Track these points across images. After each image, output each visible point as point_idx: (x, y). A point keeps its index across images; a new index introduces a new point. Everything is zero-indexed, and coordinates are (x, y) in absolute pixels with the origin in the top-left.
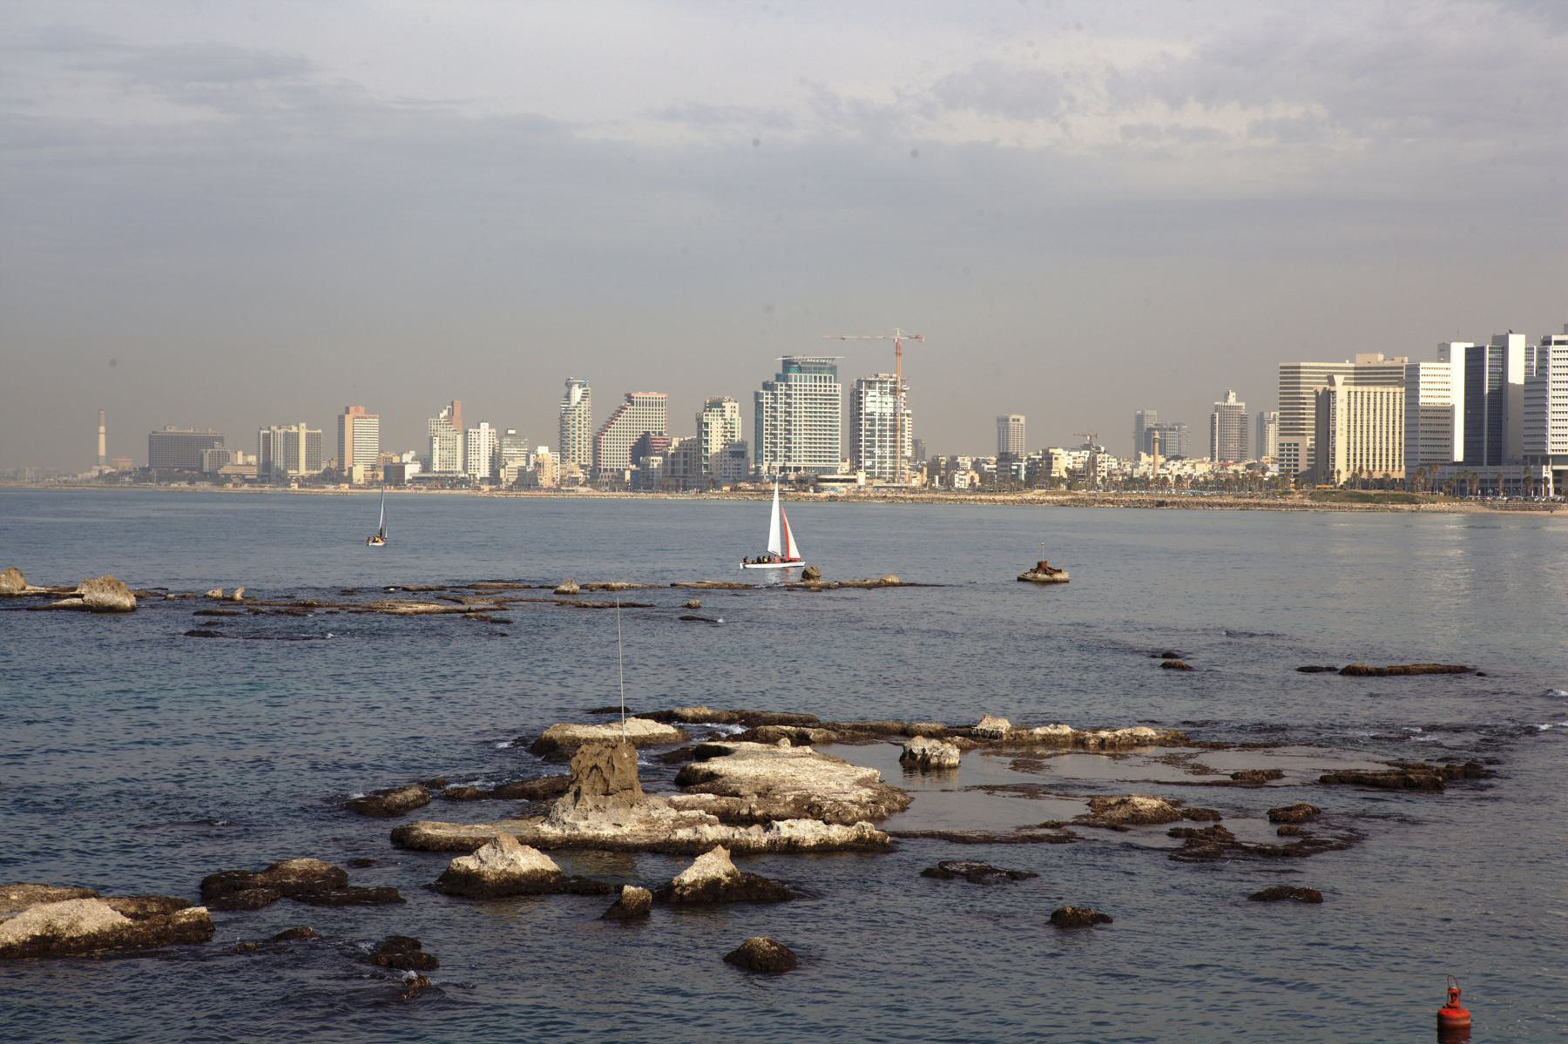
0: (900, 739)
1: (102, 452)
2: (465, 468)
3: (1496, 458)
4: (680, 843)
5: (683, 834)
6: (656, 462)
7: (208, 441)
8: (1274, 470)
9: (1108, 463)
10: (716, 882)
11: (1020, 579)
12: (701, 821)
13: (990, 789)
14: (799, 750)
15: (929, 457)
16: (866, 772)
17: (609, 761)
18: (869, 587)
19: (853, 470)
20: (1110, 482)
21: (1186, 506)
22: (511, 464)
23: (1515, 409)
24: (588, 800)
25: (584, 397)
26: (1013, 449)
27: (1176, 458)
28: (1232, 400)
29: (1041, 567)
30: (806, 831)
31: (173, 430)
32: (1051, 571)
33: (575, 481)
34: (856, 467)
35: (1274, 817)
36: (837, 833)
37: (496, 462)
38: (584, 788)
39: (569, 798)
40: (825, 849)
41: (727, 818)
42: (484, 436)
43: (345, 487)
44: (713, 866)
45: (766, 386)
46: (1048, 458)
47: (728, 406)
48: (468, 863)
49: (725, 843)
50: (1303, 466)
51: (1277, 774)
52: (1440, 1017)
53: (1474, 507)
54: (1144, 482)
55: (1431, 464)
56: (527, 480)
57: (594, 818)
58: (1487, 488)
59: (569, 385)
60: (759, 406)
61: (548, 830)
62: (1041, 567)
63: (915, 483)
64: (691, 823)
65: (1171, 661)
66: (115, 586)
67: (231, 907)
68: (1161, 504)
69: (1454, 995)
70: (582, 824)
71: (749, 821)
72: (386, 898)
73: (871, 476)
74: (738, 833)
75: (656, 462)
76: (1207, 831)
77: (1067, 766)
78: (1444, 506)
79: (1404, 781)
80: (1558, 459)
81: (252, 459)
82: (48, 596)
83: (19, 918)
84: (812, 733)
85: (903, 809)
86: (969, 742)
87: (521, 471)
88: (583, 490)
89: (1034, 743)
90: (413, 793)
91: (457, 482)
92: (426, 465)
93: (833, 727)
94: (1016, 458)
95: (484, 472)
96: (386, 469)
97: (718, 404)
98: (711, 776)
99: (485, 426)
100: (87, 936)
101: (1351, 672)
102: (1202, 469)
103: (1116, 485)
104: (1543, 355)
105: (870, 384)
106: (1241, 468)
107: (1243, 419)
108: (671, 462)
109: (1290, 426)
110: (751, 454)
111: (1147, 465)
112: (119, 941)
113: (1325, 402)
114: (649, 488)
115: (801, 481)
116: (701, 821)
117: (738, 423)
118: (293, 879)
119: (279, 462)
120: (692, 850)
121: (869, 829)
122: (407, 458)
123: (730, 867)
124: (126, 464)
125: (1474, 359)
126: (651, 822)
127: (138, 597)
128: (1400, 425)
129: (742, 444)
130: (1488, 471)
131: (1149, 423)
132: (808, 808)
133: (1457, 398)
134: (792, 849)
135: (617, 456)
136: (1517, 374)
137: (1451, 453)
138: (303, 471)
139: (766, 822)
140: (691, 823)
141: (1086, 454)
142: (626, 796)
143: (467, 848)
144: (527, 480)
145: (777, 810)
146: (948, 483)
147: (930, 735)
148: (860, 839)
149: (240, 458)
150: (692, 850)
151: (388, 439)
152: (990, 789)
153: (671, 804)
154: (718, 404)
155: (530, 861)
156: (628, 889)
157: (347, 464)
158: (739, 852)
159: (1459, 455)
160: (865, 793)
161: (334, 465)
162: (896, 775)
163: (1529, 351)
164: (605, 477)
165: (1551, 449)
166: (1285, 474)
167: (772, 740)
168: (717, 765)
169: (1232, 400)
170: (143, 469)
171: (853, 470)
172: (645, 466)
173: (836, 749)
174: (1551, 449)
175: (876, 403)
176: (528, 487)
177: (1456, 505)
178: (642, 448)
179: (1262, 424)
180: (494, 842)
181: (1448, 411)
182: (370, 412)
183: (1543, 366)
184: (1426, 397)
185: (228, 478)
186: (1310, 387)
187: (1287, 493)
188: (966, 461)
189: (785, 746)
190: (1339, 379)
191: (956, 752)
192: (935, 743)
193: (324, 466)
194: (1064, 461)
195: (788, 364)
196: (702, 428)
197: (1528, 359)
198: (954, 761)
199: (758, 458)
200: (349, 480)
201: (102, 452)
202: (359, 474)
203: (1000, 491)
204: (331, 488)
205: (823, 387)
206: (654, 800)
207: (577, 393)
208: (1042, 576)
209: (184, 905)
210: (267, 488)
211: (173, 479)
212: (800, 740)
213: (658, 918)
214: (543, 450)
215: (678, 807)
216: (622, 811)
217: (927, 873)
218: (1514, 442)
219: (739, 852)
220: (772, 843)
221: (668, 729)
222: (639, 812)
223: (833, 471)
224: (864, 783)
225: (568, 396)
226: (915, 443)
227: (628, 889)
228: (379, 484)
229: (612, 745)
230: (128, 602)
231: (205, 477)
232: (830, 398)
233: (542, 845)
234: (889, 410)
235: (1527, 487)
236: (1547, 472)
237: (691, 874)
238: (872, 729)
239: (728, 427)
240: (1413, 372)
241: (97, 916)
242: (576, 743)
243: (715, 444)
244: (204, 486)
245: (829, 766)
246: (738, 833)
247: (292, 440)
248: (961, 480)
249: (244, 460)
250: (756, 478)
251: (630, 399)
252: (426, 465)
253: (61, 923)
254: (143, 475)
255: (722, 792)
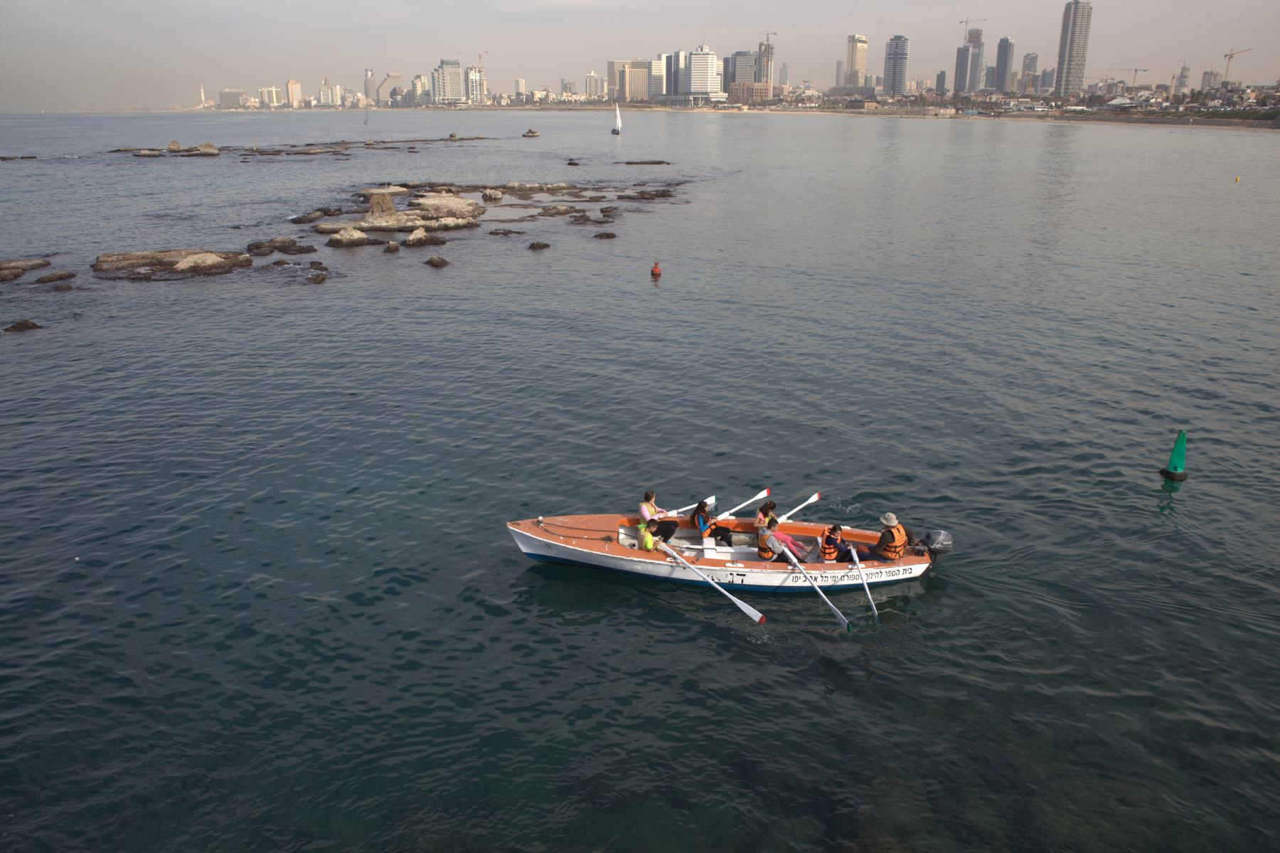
0: (482, 190)
1: (203, 98)
2: (333, 102)
3: (676, 93)
4: (409, 227)
5: (409, 224)
6: (399, 98)
7: (241, 94)
8: (606, 98)
9: (552, 96)
10: (420, 239)
11: (524, 136)
12: (415, 219)
13: (511, 206)
14: (448, 195)
15: (493, 94)
16: (470, 201)
17: (383, 200)
18: (472, 139)
19: (467, 100)
20: (553, 102)
21: (578, 110)
22: (349, 100)
23: (681, 76)
24: (377, 215)
25: (372, 75)
26: (521, 91)
27: (575, 94)
28: (592, 74)
29: (530, 131)
30: (451, 221)
31: (227, 90)
32: (533, 133)
33: (371, 105)
34: (468, 98)
35: (602, 211)
36: (461, 221)
37: (343, 99)
38: (375, 210)
39: (370, 213)
40: (457, 227)
41: (424, 218)
42: (338, 90)
43: (291, 109)
44: (419, 234)
45: (436, 70)
46: (533, 94)
47: (422, 77)
48: (337, 236)
49: (423, 226)
50: (615, 96)
51: (604, 197)
52: (652, 271)
53: (669, 109)
54: (564, 102)
55: (656, 96)
56: (355, 105)
57: (379, 220)
58: (673, 103)
59: (366, 71)
60: (433, 77)
61: (364, 225)
62: (530, 131)
63: (488, 103)
64: (412, 220)
65: (572, 163)
66: (211, 146)
67: (257, 255)
68: (570, 109)
69: (656, 264)
70: (375, 222)
71: (432, 218)
72: (310, 250)
73: (473, 101)
74: (427, 223)
75: (399, 98)
76: (581, 216)
77: (538, 197)
78: (660, 109)
79: (644, 197)
80: (694, 93)
81: (257, 100)
82: (187, 151)
83: (185, 260)
84: (453, 189)
85: (483, 213)
86: (505, 190)
87: (352, 102)
88: (375, 108)
89: (526, 190)
90: (318, 213)
91: (330, 107)
92: (319, 101)
93: (460, 187)
94: (522, 94)
95: (339, 103)
96: (305, 103)
97: (419, 77)
98: (419, 204)
99: (338, 86)
100: (209, 266)
101: (628, 163)
102: (583, 98)
103: (555, 103)
104: (690, 58)
105: (471, 69)
106: (596, 97)
107: (596, 80)
108: (404, 98)
109: (611, 83)
110: (432, 94)
111: (565, 96)
112: (220, 266)
113: (622, 73)
114: (397, 107)
115: (449, 103)
116: (415, 219)
117: (426, 83)
118: (278, 244)
119: (267, 101)
120: (411, 230)
121: (471, 220)
122: (311, 98)
123: (425, 234)
124: (212, 103)
125: (669, 59)
126: (399, 220)
127: (220, 150)
128: (646, 82)
129: (428, 91)
130: (673, 97)
131: (565, 82)
132: (451, 214)
133: (664, 73)
134: (446, 228)
135: (385, 96)
136: (682, 65)
137: (662, 89)
138: (275, 104)
139: (437, 219)
140: (412, 220)
141: (545, 93)
142: (389, 212)
143: (336, 232)
144: (355, 105)
145: (441, 215)
146: (499, 103)
147: (492, 188)
148: (468, 223)
149: (253, 100)
150: (411, 230)
151: (303, 91)
152: (511, 206)
153: (405, 214)
154: (419, 77)
155: (358, 235)
156: (391, 242)
157: (291, 101)
158: (428, 229)
159: (664, 92)
160: (470, 208)
161: (286, 101)
162: (481, 202)
163: (686, 57)
164: (382, 104)
165: (692, 90)
166: (610, 99)
167: (439, 192)
168: (421, 201)
169: (592, 74)
170: (219, 105)
171: (467, 100)
172: (395, 100)
173: (462, 194)
174: (692, 90)
175: (474, 76)
176: (355, 108)
177: (664, 109)
178: (394, 93)
179: (602, 82)
180: (345, 229)
181: (661, 77)
182: (297, 82)
183: (690, 60)
184: (654, 73)
185: (249, 107)
186: (617, 69)
187: (610, 105)
188: (505, 96)
189: (444, 194)
190: (626, 66)
191: (500, 193)
192: (493, 191)
193: (283, 102)
194: (538, 95)
195: (442, 62)
196: (414, 85)
197: (686, 60)
198: (500, 196)
199: (434, 95)
200: (292, 107)
201: (203, 98)
202: (295, 104)
203: (517, 106)
204: (286, 110)
205: (455, 70)
206: (399, 213)
207: (370, 74)
208: (530, 134)
209: (241, 254)
210: (263, 110)
211: (229, 108)
212: (449, 191)
213: (403, 251)
214: (359, 95)
215: (408, 215)
216: (388, 217)
217: (491, 233)
218: (682, 89)
219: (428, 229)
220: (439, 226)
221: (405, 189)
222: (394, 217)
223: (460, 100)
224: (470, 205)
225: (366, 75)
226: (488, 89)
227: (391, 242)
228: (303, 108)
229: (383, 195)
230: (216, 152)
231: (241, 107)
232: (458, 74)
233: (362, 230)
234: (478, 78)
235: (685, 103)
236: (691, 98)
237: (412, 237)
238: (473, 187)
239: (423, 85)
240: (650, 63)
241: (211, 259)
242: (373, 194)
243: (419, 91)
244: (241, 110)
245: (458, 200)
246: (427, 223)
247: (270, 93)
248: (504, 102)
249: (254, 101)
250: (434, 103)
251: (388, 75)
252: (319, 101)
253: (200, 261)
254: (219, 107)
255: (422, 210)
